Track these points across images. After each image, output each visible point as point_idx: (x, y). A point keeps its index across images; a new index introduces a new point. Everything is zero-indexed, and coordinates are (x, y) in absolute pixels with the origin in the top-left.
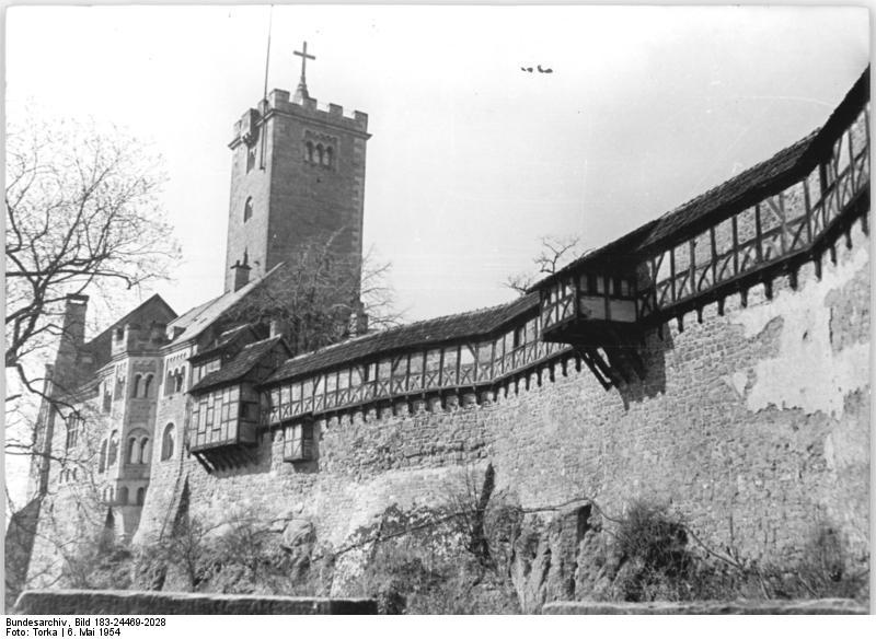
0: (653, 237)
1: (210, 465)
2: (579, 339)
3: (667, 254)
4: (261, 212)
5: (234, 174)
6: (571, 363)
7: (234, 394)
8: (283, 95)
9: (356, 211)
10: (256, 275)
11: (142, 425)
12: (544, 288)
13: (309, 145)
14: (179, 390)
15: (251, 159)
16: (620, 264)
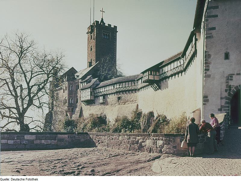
0: (164, 64)
1: (86, 104)
2: (150, 82)
3: (164, 68)
4: (94, 49)
5: (88, 40)
6: (150, 86)
7: (89, 90)
8: (97, 22)
9: (115, 49)
10: (94, 64)
11: (71, 96)
12: (143, 73)
13: (104, 34)
14: (79, 88)
15: (91, 36)
16: (157, 68)
